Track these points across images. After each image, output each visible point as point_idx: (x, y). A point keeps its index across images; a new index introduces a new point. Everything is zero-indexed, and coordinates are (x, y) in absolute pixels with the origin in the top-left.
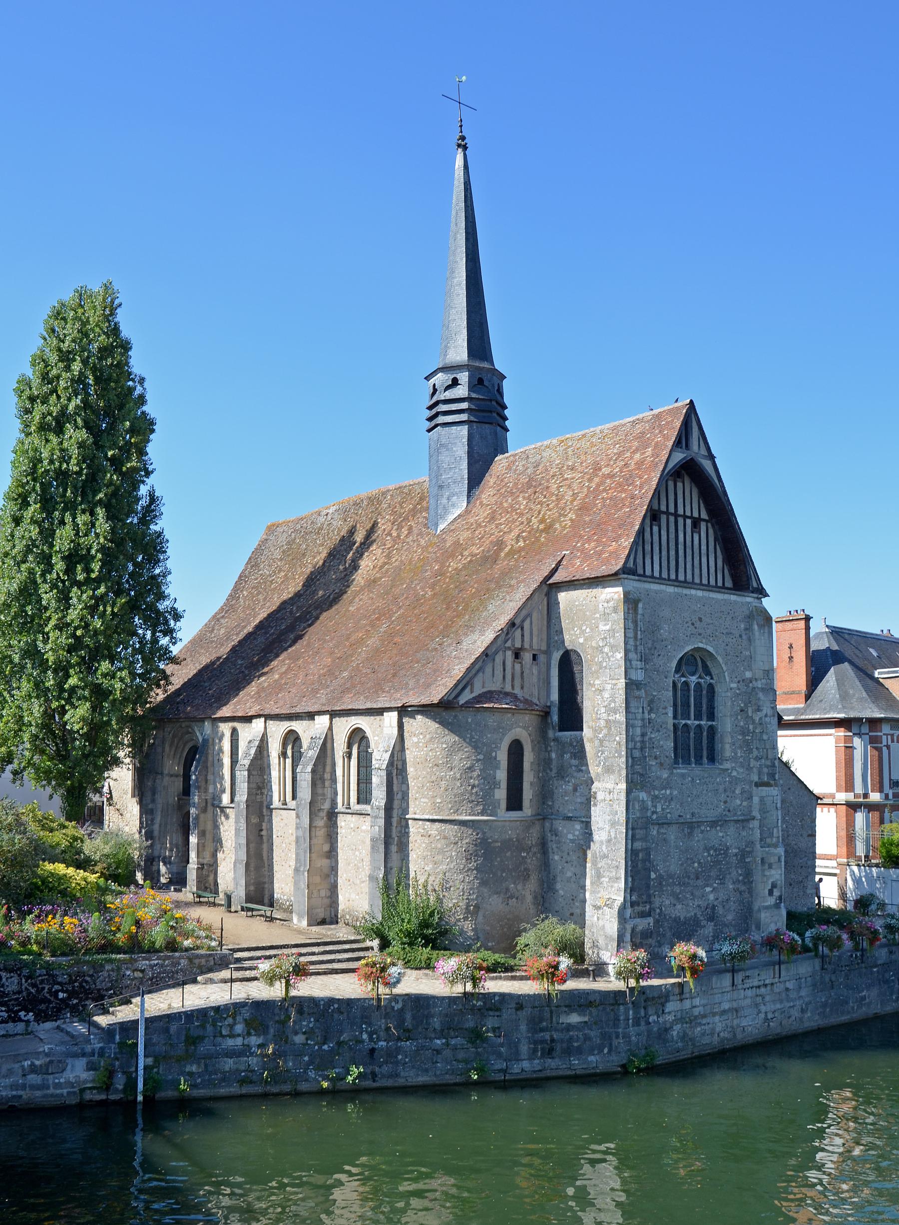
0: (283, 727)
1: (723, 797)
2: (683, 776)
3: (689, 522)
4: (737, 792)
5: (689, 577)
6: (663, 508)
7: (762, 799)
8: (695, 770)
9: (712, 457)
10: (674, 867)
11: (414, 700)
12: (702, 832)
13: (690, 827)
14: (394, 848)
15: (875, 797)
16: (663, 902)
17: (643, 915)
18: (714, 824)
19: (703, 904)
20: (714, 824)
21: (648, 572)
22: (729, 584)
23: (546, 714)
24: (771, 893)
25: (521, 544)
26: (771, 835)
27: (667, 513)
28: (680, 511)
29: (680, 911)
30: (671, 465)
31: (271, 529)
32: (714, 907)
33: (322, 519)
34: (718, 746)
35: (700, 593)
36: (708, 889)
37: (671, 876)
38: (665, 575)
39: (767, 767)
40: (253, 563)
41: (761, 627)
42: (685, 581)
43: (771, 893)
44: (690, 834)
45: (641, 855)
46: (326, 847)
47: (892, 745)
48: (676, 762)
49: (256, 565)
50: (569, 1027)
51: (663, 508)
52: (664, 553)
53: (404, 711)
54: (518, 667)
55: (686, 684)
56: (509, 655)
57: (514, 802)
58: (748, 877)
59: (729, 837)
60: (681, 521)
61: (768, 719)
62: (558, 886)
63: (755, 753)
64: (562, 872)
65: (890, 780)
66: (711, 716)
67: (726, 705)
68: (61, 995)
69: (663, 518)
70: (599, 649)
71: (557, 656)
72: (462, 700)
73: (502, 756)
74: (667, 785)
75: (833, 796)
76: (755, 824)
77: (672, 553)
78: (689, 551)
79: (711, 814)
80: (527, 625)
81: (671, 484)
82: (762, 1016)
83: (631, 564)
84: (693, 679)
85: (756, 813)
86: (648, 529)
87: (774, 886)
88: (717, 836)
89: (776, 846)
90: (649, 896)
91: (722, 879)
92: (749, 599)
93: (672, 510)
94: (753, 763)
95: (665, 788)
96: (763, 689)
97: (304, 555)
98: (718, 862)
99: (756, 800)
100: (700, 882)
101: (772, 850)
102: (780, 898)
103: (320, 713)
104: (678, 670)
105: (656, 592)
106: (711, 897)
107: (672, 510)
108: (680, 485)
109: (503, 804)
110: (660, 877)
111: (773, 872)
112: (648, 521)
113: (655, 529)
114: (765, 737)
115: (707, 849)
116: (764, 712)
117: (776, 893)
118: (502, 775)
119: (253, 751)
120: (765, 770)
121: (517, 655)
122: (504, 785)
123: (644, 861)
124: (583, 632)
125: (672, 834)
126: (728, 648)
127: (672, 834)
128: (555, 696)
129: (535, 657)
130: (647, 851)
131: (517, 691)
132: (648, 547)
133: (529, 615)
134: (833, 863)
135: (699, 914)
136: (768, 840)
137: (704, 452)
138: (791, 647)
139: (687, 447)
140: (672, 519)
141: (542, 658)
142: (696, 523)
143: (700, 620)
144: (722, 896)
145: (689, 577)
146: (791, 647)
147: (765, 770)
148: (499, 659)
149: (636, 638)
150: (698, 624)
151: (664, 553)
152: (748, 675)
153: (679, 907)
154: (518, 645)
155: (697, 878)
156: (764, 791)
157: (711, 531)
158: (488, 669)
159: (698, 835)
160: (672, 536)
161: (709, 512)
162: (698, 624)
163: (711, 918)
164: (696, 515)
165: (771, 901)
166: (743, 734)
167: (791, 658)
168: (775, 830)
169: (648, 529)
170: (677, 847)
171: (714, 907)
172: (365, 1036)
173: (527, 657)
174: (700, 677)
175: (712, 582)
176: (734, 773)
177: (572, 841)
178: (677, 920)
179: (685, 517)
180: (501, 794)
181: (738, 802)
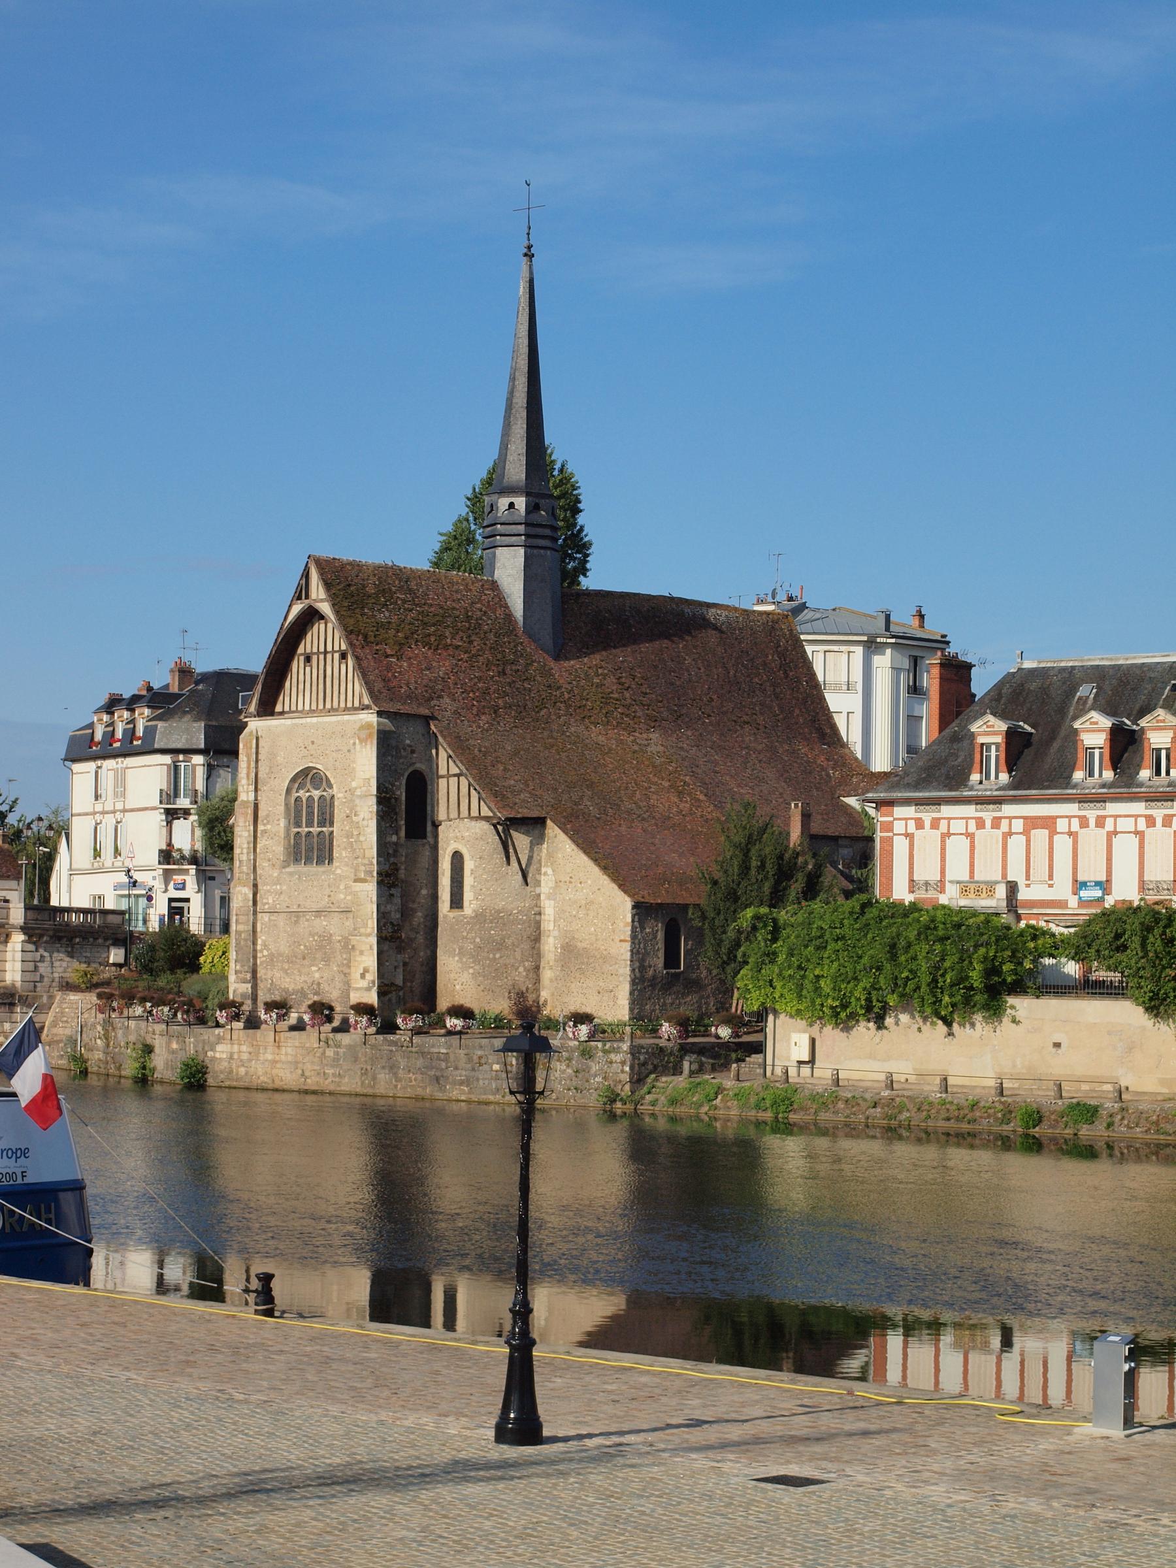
1: (327, 892)
2: (291, 874)
3: (337, 656)
4: (342, 887)
6: (315, 650)
8: (313, 869)
10: (284, 948)
12: (307, 920)
13: (296, 915)
18: (319, 913)
19: (310, 981)
20: (319, 913)
21: (300, 708)
24: (363, 976)
28: (329, 648)
30: (291, 618)
35: (314, 720)
36: (314, 968)
37: (280, 955)
39: (365, 865)
41: (361, 741)
42: (346, 709)
43: (363, 976)
44: (296, 922)
47: (918, 834)
48: (286, 864)
52: (314, 688)
55: (310, 799)
59: (334, 926)
60: (329, 656)
61: (365, 823)
65: (912, 881)
67: (339, 814)
69: (315, 658)
74: (278, 881)
79: (315, 907)
84: (316, 794)
86: (301, 671)
87: (366, 970)
88: (321, 924)
89: (369, 935)
91: (327, 960)
92: (361, 716)
96: (360, 797)
100: (306, 962)
101: (363, 938)
105: (276, 727)
106: (317, 975)
107: (322, 649)
110: (271, 956)
111: (364, 958)
113: (308, 669)
114: (362, 838)
115: (312, 935)
116: (362, 816)
120: (363, 868)
125: (281, 920)
126: (337, 764)
127: (281, 920)
132: (301, 686)
135: (306, 988)
136: (362, 930)
139: (307, 597)
140: (322, 657)
142: (343, 656)
143: (313, 743)
145: (335, 705)
147: (363, 868)
150: (310, 747)
151: (314, 688)
152: (354, 784)
153: (288, 980)
155: (304, 958)
156: (359, 886)
159: (303, 923)
160: (321, 672)
162: (310, 747)
164: (344, 647)
165: (363, 984)
166: (348, 837)
168: (370, 922)
170: (285, 931)
171: (319, 984)
174: (325, 790)
176: (339, 871)
181: (342, 896)
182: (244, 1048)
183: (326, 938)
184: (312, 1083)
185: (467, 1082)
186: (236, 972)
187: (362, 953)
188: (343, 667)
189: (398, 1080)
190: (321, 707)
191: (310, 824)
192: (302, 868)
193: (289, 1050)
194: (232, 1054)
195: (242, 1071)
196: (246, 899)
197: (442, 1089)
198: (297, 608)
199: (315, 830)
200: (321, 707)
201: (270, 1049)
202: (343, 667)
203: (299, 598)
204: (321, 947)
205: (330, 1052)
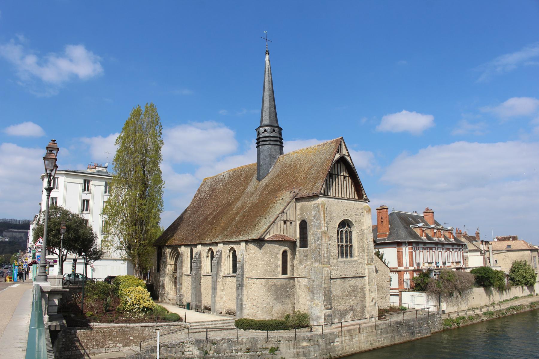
0: (207, 248)
1: (355, 269)
3: (342, 177)
5: (343, 196)
7: (368, 270)
9: (349, 155)
11: (250, 238)
14: (244, 288)
15: (411, 268)
16: (335, 304)
17: (328, 309)
22: (356, 197)
23: (295, 243)
24: (372, 301)
25: (287, 185)
26: (372, 281)
27: (335, 174)
28: (339, 174)
29: (341, 308)
30: (335, 158)
31: (205, 180)
32: (353, 306)
33: (222, 177)
34: (353, 252)
37: (338, 296)
38: (334, 195)
40: (199, 191)
41: (367, 212)
43: (372, 301)
44: (344, 282)
45: (327, 289)
46: (222, 288)
49: (200, 193)
50: (303, 347)
51: (334, 173)
53: (247, 242)
54: (285, 226)
56: (282, 222)
57: (284, 272)
58: (364, 297)
60: (339, 177)
62: (300, 300)
63: (366, 254)
64: (301, 295)
66: (351, 242)
68: (131, 338)
69: (334, 176)
70: (311, 220)
71: (298, 223)
72: (266, 238)
73: (280, 256)
75: (397, 268)
76: (366, 278)
77: (337, 187)
78: (342, 187)
80: (288, 212)
81: (336, 165)
82: (370, 342)
83: (322, 192)
84: (344, 230)
85: (366, 274)
86: (328, 180)
87: (373, 299)
88: (353, 282)
89: (374, 285)
90: (331, 303)
91: (356, 297)
93: (336, 173)
94: (366, 257)
95: (335, 266)
97: (216, 189)
98: (355, 291)
99: (367, 270)
102: (376, 303)
103: (220, 243)
104: (339, 226)
106: (352, 303)
107: (336, 173)
108: (339, 165)
109: (281, 273)
112: (328, 177)
115: (350, 287)
117: (374, 301)
118: (280, 263)
119: (197, 256)
121: (285, 222)
122: (281, 266)
123: (328, 291)
124: (307, 214)
128: (298, 236)
129: (291, 223)
130: (330, 287)
131: (285, 234)
133: (289, 209)
134: (397, 291)
137: (347, 154)
138: (382, 218)
141: (293, 223)
142: (345, 177)
144: (355, 302)
146: (382, 218)
148: (279, 224)
149: (324, 216)
152: (363, 228)
154: (285, 219)
157: (350, 180)
158: (275, 226)
161: (349, 174)
163: (352, 310)
164: (345, 175)
165: (373, 304)
167: (382, 222)
169: (328, 180)
171: (353, 306)
172: (234, 351)
173: (288, 223)
175: (351, 197)
177: (305, 285)
178: (340, 311)
179: (341, 176)
180: (280, 269)
182: (347, 338)
183: (355, 287)
184: (375, 346)
185: (420, 332)
186: (324, 306)
187: (372, 292)
188: (345, 182)
189: (402, 336)
190: (337, 195)
191: (342, 242)
192: (340, 259)
193: (365, 335)
194: (342, 342)
195: (347, 348)
196: (328, 273)
197: (414, 337)
198: (337, 156)
199: (344, 244)
200: (337, 195)
201: (357, 336)
202: (345, 182)
203: (338, 152)
204: (353, 291)
205: (379, 332)
